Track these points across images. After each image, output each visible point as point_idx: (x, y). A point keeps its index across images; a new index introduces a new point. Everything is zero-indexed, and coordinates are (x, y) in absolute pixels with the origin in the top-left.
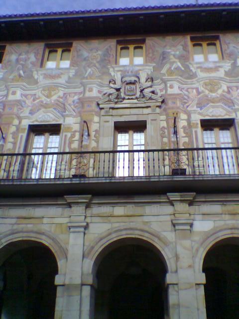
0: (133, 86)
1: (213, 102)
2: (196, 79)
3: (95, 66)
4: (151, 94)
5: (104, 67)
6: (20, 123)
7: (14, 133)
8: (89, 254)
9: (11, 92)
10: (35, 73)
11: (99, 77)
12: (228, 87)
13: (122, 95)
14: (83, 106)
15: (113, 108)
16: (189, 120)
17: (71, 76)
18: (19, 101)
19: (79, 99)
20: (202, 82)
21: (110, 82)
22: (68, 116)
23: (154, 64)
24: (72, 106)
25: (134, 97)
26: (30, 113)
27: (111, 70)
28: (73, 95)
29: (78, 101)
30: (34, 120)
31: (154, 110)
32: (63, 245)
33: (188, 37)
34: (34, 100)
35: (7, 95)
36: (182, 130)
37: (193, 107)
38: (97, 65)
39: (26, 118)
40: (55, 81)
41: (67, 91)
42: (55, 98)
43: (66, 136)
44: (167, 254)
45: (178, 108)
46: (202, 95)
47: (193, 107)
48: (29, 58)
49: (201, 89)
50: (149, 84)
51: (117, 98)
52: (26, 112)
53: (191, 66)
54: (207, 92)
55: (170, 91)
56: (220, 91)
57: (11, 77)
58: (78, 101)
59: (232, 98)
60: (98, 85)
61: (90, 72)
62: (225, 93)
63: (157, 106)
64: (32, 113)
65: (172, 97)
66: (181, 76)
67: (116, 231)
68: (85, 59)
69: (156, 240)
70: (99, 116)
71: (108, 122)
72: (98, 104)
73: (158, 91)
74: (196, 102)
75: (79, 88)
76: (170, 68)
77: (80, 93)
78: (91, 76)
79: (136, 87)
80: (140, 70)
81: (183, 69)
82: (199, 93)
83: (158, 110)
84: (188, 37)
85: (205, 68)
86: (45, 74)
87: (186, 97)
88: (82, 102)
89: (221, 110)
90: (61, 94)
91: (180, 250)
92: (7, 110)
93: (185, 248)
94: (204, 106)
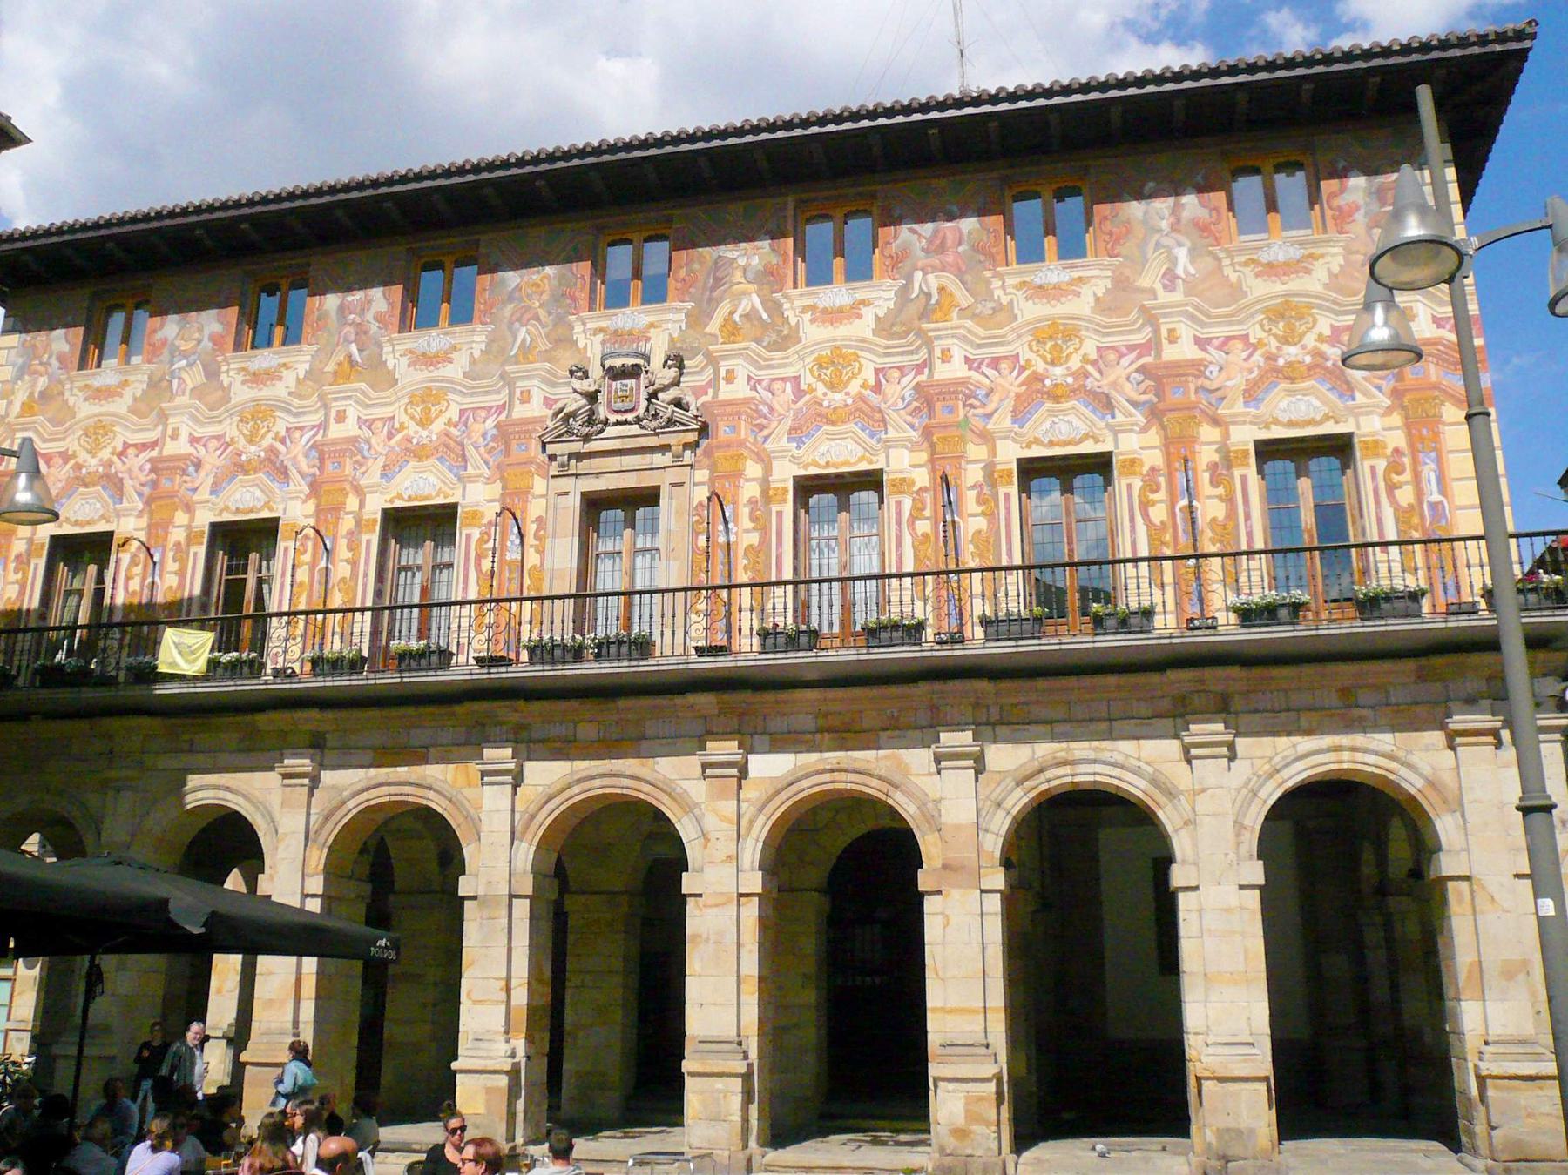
0: (631, 383)
1: (833, 423)
2: (798, 347)
3: (538, 320)
4: (672, 407)
5: (560, 320)
6: (362, 505)
7: (350, 533)
8: (527, 827)
9: (333, 414)
10: (387, 349)
11: (547, 356)
12: (877, 371)
13: (602, 412)
14: (507, 451)
15: (579, 456)
16: (765, 483)
17: (477, 354)
18: (354, 440)
19: (498, 426)
20: (809, 360)
21: (572, 373)
22: (474, 479)
23: (689, 305)
24: (482, 450)
25: (630, 417)
26: (383, 476)
27: (578, 328)
28: (483, 414)
29: (494, 432)
30: (394, 494)
31: (678, 456)
32: (472, 811)
33: (790, 201)
34: (390, 436)
35: (323, 426)
36: (746, 510)
37: (779, 442)
38: (542, 313)
39: (374, 489)
40: (436, 373)
41: (469, 402)
42: (439, 425)
43: (468, 537)
44: (686, 830)
45: (742, 444)
46: (808, 397)
47: (779, 442)
48: (370, 302)
49: (807, 380)
50: (673, 372)
51: (591, 420)
52: (372, 476)
53: (786, 306)
54: (821, 389)
55: (726, 392)
56: (854, 387)
57: (330, 367)
58: (494, 432)
59: (883, 406)
60: (545, 381)
61: (524, 340)
62: (867, 392)
63: (686, 446)
64: (387, 472)
65: (728, 409)
66: (758, 341)
67: (580, 781)
68: (510, 299)
69: (665, 799)
70: (545, 476)
71: (566, 493)
72: (544, 445)
73: (689, 398)
74: (788, 423)
75: (498, 392)
76: (732, 313)
77: (501, 408)
78: (526, 352)
79: (638, 386)
80: (652, 325)
81: (765, 316)
82: (799, 393)
83: (688, 456)
84: (790, 201)
85: (825, 311)
86: (411, 352)
87: (765, 410)
88: (506, 434)
89: (851, 445)
90: (453, 413)
91: (710, 822)
92: (330, 467)
93: (723, 819)
94: (809, 436)
